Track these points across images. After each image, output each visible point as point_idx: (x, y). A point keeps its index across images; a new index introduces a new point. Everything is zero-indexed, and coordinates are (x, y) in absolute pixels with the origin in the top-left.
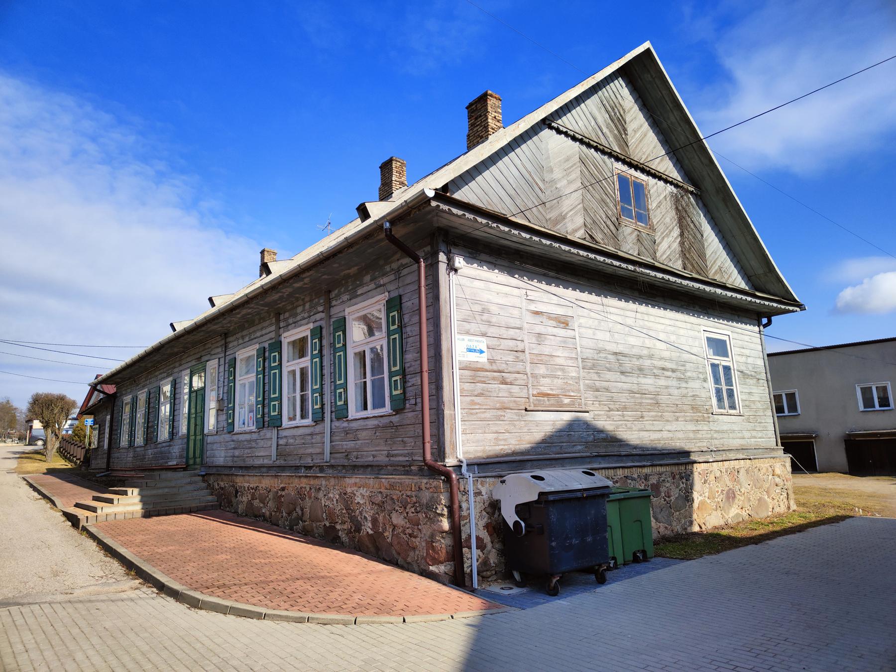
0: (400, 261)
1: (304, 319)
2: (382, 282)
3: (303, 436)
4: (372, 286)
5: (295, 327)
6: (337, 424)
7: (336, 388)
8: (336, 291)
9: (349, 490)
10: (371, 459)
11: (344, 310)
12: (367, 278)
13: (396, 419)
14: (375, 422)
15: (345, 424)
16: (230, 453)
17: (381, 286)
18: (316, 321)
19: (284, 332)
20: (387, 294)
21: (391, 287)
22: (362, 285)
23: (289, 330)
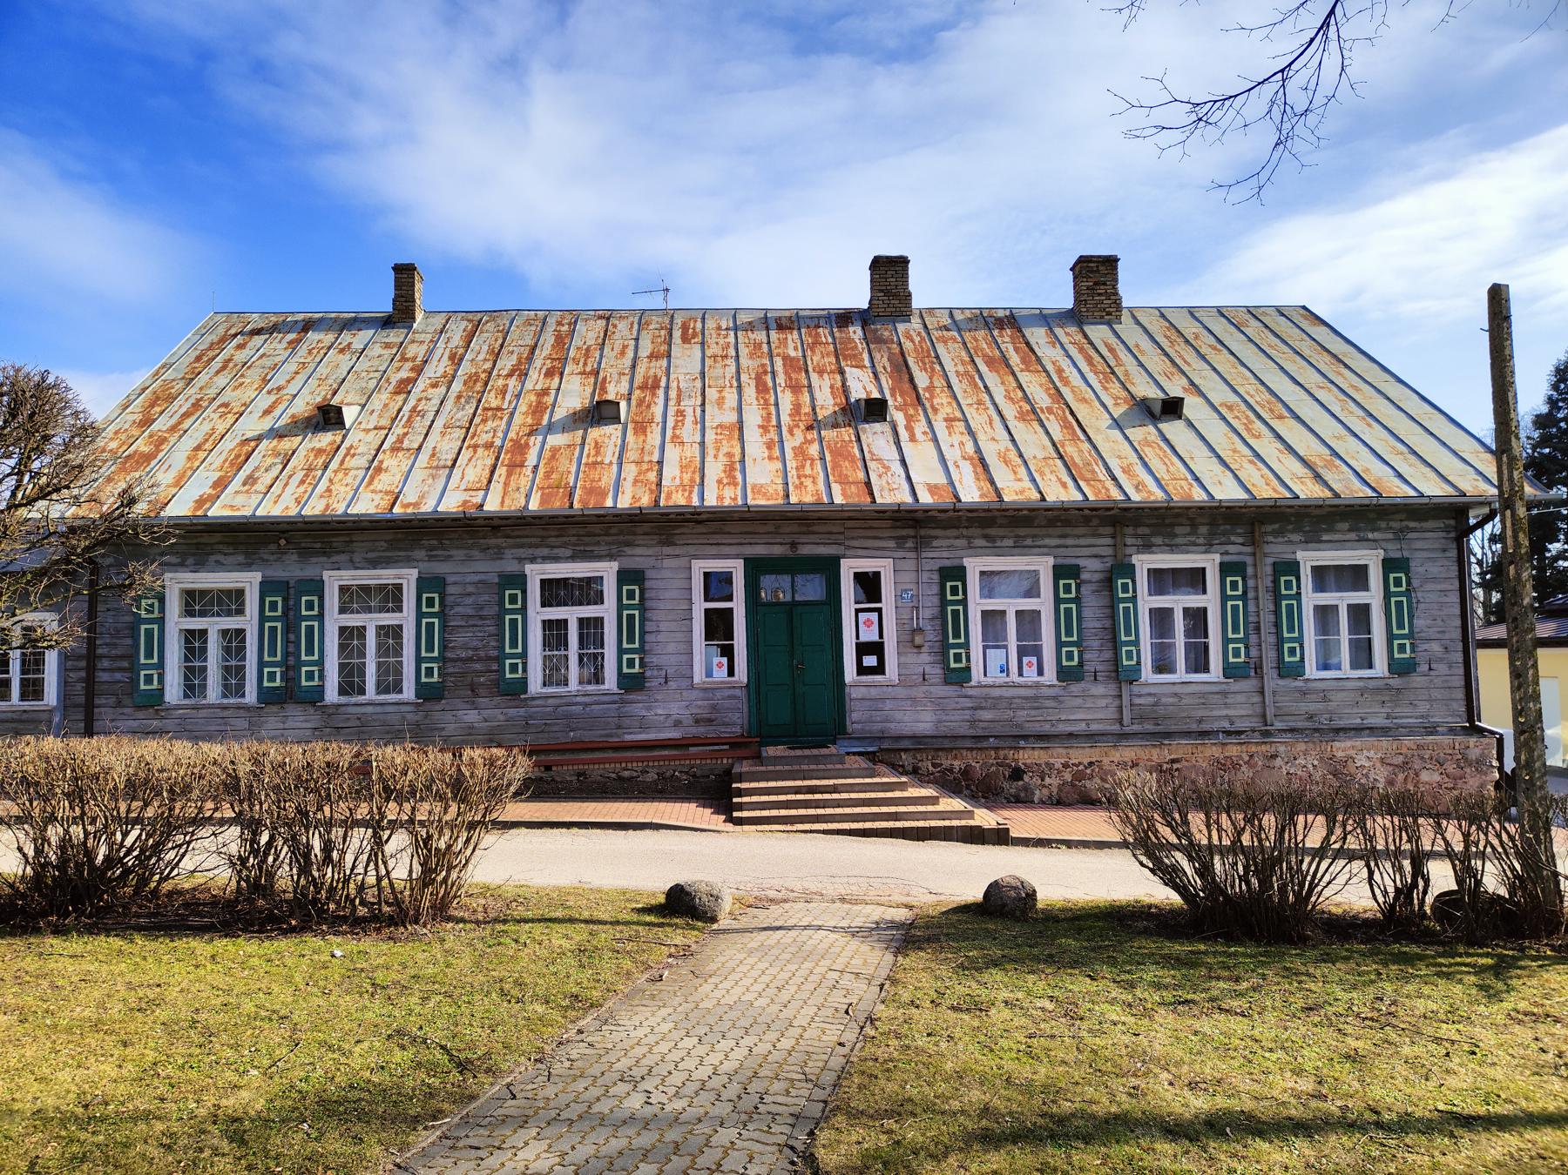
2: (1370, 536)
3: (1203, 695)
4: (1353, 536)
5: (1172, 552)
6: (1282, 682)
9: (1340, 754)
10: (1359, 721)
11: (1294, 553)
12: (1346, 526)
13: (1396, 682)
14: (1361, 684)
16: (967, 715)
18: (1227, 553)
19: (1138, 552)
20: (1382, 551)
21: (1390, 546)
22: (1331, 530)
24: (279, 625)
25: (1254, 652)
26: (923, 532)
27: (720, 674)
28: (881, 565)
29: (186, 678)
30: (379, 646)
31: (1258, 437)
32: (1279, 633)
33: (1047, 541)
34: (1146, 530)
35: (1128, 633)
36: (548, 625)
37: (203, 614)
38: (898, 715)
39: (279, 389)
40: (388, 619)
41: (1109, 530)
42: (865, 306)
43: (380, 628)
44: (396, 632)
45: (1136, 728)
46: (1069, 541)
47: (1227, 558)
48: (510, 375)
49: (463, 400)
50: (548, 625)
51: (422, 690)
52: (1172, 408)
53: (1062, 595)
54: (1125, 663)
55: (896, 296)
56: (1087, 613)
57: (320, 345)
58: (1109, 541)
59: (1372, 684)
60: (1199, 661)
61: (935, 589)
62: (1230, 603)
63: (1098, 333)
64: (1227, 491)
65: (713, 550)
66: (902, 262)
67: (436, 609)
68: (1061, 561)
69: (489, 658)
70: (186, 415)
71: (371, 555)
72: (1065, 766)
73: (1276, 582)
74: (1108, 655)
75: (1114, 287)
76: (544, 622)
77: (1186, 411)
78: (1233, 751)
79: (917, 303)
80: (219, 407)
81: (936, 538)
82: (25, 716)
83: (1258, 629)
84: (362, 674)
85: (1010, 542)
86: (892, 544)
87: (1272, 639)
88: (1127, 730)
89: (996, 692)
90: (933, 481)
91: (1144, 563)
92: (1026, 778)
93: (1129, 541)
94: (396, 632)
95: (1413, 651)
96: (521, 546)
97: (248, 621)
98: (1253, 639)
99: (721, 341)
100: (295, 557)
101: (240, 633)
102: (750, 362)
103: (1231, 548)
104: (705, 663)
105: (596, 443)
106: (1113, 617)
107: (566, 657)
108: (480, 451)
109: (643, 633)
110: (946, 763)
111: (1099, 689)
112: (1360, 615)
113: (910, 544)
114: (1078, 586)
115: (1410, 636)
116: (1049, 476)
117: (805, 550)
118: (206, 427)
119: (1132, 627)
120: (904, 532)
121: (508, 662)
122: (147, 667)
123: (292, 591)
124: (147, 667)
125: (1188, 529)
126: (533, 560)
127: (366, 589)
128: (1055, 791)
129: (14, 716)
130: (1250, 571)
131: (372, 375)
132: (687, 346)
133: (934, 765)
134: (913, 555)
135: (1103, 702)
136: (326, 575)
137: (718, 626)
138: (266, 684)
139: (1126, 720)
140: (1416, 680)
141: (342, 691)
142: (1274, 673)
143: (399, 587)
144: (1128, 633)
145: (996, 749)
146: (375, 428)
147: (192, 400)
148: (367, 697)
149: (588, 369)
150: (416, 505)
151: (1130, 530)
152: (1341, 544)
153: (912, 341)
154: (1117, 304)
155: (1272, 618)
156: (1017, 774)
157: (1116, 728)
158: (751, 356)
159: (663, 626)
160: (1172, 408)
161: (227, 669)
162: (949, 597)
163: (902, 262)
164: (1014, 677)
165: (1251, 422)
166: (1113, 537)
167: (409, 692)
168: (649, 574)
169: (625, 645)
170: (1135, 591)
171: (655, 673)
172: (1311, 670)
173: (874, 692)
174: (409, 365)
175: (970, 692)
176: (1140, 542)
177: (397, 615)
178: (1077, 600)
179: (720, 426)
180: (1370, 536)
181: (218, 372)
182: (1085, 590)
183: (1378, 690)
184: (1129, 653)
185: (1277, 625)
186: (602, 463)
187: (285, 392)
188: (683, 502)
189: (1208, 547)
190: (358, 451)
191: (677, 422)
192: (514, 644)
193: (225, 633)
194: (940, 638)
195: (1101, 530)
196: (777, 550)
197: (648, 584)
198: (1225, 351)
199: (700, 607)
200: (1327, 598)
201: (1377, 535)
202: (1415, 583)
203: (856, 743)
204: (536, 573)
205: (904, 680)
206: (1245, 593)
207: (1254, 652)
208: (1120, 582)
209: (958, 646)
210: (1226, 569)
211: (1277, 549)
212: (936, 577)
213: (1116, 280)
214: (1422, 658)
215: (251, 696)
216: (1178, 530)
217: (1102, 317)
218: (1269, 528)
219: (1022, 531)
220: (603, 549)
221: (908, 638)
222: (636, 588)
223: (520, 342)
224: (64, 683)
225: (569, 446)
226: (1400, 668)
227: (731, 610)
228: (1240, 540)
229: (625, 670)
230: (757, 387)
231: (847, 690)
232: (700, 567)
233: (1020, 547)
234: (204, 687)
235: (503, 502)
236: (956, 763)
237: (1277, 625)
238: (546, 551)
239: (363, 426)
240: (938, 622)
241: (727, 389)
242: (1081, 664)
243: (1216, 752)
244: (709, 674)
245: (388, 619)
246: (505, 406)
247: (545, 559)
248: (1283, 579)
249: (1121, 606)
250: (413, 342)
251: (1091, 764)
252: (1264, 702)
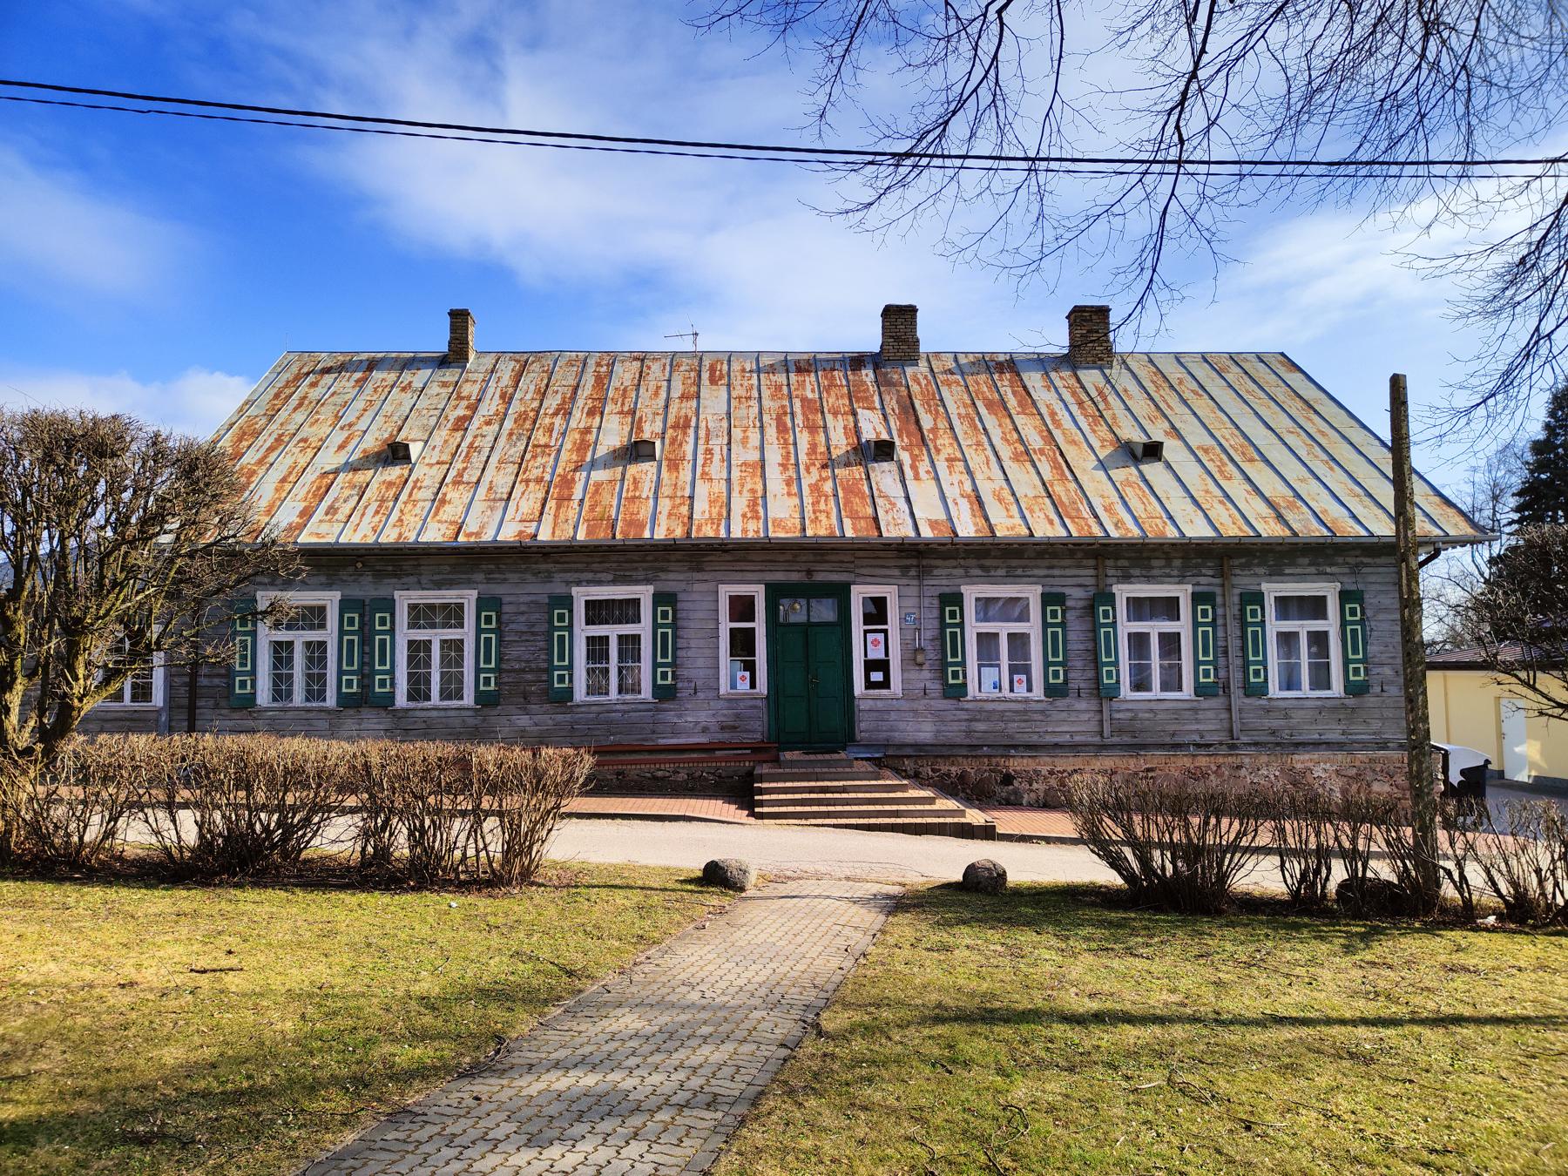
0: (1359, 559)
2: (1329, 570)
3: (1176, 711)
4: (1312, 570)
5: (1149, 582)
6: (1247, 701)
8: (1243, 560)
9: (1299, 766)
10: (1317, 736)
11: (1260, 584)
12: (1306, 561)
13: (1351, 702)
14: (1319, 703)
17: (1326, 574)
18: (1198, 584)
19: (1118, 583)
21: (1345, 579)
22: (1293, 564)
23: (1131, 583)
24: (356, 638)
25: (1222, 674)
26: (925, 562)
27: (743, 686)
28: (889, 592)
29: (275, 684)
30: (442, 658)
31: (1229, 479)
32: (1245, 656)
33: (1036, 572)
34: (1126, 563)
35: (1108, 655)
36: (591, 640)
38: (902, 725)
39: (350, 425)
40: (452, 634)
41: (1092, 562)
42: (877, 350)
43: (443, 642)
44: (458, 645)
45: (1115, 740)
46: (1056, 572)
48: (556, 414)
49: (514, 437)
50: (591, 640)
51: (480, 696)
52: (1153, 451)
53: (1049, 620)
54: (1105, 681)
55: (904, 341)
56: (1071, 636)
57: (384, 384)
58: (1092, 572)
59: (1329, 704)
60: (1172, 681)
61: (936, 613)
62: (1200, 629)
63: (1091, 377)
64: (1197, 529)
65: (739, 576)
66: (911, 311)
67: (493, 626)
68: (1048, 589)
69: (540, 670)
70: (271, 449)
71: (436, 577)
72: (1051, 773)
73: (1242, 611)
74: (1090, 674)
76: (588, 638)
77: (1165, 453)
78: (1202, 761)
79: (924, 348)
80: (299, 442)
81: (937, 567)
82: (136, 715)
83: (1226, 653)
84: (428, 682)
85: (1001, 572)
86: (896, 572)
87: (1239, 662)
88: (1107, 741)
89: (990, 706)
90: (933, 518)
91: (1123, 592)
92: (1016, 783)
93: (1111, 572)
94: (458, 645)
95: (1366, 673)
96: (569, 571)
97: (329, 635)
98: (1222, 661)
99: (746, 384)
100: (370, 579)
101: (322, 645)
102: (771, 403)
103: (1203, 580)
104: (729, 677)
105: (635, 479)
106: (1095, 640)
107: (607, 670)
108: (532, 485)
109: (675, 649)
110: (944, 769)
111: (1082, 705)
112: (1319, 639)
113: (913, 572)
114: (1064, 612)
115: (1364, 661)
116: (1038, 513)
117: (820, 577)
118: (289, 461)
119: (1112, 649)
120: (908, 562)
121: (556, 673)
123: (367, 608)
125: (1162, 563)
126: (579, 583)
127: (431, 607)
128: (1042, 795)
129: (126, 715)
130: (1219, 600)
131: (432, 412)
132: (714, 387)
133: (933, 770)
134: (915, 582)
135: (1086, 717)
136: (397, 594)
137: (742, 644)
138: (344, 690)
139: (1105, 735)
140: (1370, 700)
141: (410, 697)
142: (1241, 692)
143: (461, 606)
144: (1108, 655)
145: (989, 757)
146: (438, 463)
147: (275, 436)
148: (432, 702)
149: (626, 409)
150: (478, 534)
151: (1110, 563)
152: (1301, 578)
153: (919, 384)
154: (1109, 351)
155: (1238, 643)
156: (1008, 779)
157: (1097, 739)
158: (773, 397)
159: (693, 644)
160: (1153, 451)
161: (309, 676)
162: (948, 621)
163: (911, 311)
164: (1006, 692)
165: (1224, 464)
167: (469, 699)
168: (681, 597)
169: (659, 660)
170: (1115, 617)
171: (686, 684)
172: (1274, 690)
173: (880, 704)
174: (464, 403)
175: (967, 706)
176: (1119, 573)
177: (459, 630)
178: (1063, 625)
179: (744, 464)
180: (1329, 570)
181: (295, 409)
182: (1070, 616)
183: (1334, 709)
184: (1109, 673)
185: (1244, 648)
186: (639, 497)
187: (355, 428)
188: (711, 534)
189: (1181, 579)
190: (424, 484)
191: (706, 459)
192: (561, 658)
193: (308, 644)
194: (939, 657)
195: (1085, 562)
196: (795, 577)
197: (679, 606)
198: (1206, 397)
199: (726, 626)
200: (1289, 626)
201: (1334, 569)
202: (1369, 613)
203: (862, 749)
204: (582, 595)
205: (907, 695)
206: (1214, 619)
207: (1222, 674)
208: (1101, 609)
209: (956, 664)
210: (1197, 598)
212: (936, 602)
214: (1374, 680)
215: (331, 701)
216: (1155, 563)
217: (1094, 362)
218: (1237, 562)
219: (1014, 562)
220: (641, 574)
221: (909, 655)
222: (669, 609)
223: (564, 383)
224: (170, 686)
225: (610, 481)
226: (1355, 690)
227: (753, 629)
228: (1210, 572)
229: (659, 682)
230: (777, 427)
231: (856, 702)
232: (726, 591)
233: (1011, 577)
234: (289, 694)
235: (553, 533)
236: (953, 769)
237: (1244, 648)
238: (590, 576)
239: (427, 461)
240: (938, 643)
241: (751, 429)
242: (1066, 681)
243: (1187, 762)
244: (733, 686)
245: (452, 634)
246: (552, 444)
247: (590, 583)
248: (1249, 608)
249: (1102, 630)
250: (467, 381)
252: (1231, 718)
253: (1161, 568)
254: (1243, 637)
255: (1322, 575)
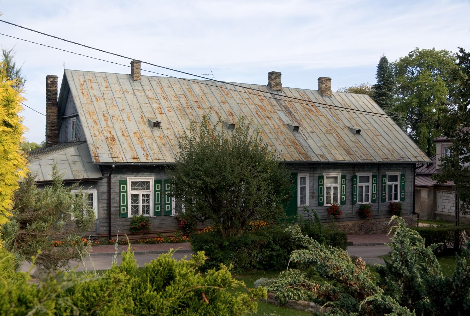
1: (368, 170)
5: (363, 172)
7: (382, 193)
15: (385, 204)
19: (357, 172)
24: (160, 193)
25: (377, 197)
28: (307, 176)
32: (382, 192)
37: (137, 189)
47: (374, 174)
61: (317, 181)
66: (279, 74)
72: (342, 226)
75: (330, 87)
77: (361, 133)
87: (381, 193)
90: (320, 154)
91: (359, 174)
97: (151, 192)
98: (377, 193)
103: (374, 171)
115: (404, 192)
122: (123, 206)
124: (123, 206)
134: (313, 172)
144: (355, 193)
155: (381, 188)
163: (279, 74)
166: (353, 168)
178: (345, 184)
202: (406, 179)
207: (377, 197)
210: (374, 176)
211: (382, 172)
213: (330, 85)
221: (311, 194)
231: (298, 208)
251: (347, 225)
253: (367, 168)
254: (382, 187)
255: (398, 170)
